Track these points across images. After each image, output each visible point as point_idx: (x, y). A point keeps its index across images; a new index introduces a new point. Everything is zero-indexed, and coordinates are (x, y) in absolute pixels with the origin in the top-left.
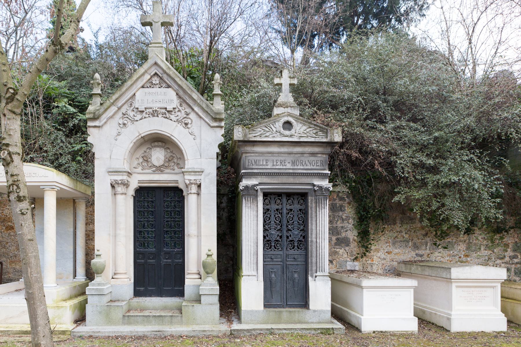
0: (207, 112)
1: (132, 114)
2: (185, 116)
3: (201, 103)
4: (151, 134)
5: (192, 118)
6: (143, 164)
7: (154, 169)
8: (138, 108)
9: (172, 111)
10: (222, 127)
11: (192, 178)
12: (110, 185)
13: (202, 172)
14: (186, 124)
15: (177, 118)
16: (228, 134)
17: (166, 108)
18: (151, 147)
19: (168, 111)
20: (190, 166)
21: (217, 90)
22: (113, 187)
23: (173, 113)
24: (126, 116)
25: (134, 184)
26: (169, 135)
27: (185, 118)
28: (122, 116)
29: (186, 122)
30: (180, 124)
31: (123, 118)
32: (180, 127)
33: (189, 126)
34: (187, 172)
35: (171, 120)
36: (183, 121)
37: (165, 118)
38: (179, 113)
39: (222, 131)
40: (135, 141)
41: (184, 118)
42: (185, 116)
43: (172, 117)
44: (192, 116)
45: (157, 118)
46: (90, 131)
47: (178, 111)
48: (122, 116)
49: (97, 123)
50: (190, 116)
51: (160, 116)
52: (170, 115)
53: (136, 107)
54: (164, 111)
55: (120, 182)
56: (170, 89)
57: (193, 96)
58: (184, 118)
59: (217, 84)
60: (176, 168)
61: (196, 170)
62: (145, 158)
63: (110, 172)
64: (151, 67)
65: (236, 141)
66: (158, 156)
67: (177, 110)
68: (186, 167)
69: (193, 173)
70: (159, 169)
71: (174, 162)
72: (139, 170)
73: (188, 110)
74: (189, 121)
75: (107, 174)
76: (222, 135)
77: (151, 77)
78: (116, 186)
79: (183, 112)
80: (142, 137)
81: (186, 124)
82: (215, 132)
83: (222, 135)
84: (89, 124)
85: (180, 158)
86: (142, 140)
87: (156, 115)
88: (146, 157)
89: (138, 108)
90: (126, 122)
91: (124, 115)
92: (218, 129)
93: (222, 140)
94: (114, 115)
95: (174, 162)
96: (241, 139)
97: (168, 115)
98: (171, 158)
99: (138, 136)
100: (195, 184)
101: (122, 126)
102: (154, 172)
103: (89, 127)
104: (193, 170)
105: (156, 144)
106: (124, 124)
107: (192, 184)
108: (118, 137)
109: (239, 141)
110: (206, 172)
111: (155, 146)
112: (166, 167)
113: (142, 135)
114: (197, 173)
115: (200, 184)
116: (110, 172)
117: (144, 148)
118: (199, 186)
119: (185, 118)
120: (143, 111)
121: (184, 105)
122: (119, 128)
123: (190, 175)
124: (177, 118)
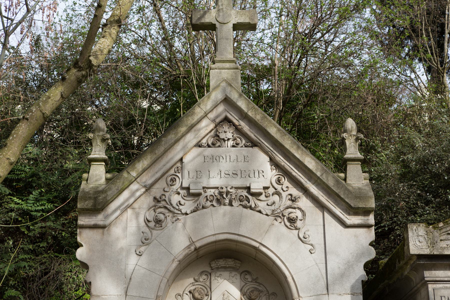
0: (339, 196)
2: (289, 203)
3: (324, 178)
4: (216, 242)
8: (188, 189)
9: (260, 194)
10: (368, 226)
14: (292, 221)
15: (273, 208)
16: (388, 239)
17: (248, 188)
18: (210, 271)
19: (253, 194)
21: (352, 150)
23: (262, 197)
24: (163, 203)
26: (257, 245)
28: (153, 203)
29: (293, 216)
30: (279, 220)
32: (280, 228)
33: (299, 224)
35: (260, 212)
36: (286, 213)
37: (245, 207)
39: (370, 235)
40: (181, 257)
41: (287, 208)
43: (262, 205)
44: (304, 202)
45: (228, 208)
46: (83, 237)
48: (153, 203)
49: (98, 219)
51: (235, 204)
52: (258, 203)
53: (185, 185)
54: (245, 193)
56: (256, 149)
57: (306, 163)
59: (353, 139)
62: (197, 295)
64: (216, 106)
65: (413, 255)
67: (271, 190)
73: (295, 192)
74: (298, 214)
76: (371, 244)
77: (216, 127)
79: (284, 194)
80: (196, 249)
83: (371, 244)
84: (82, 221)
85: (274, 294)
87: (227, 201)
89: (188, 189)
90: (162, 217)
91: (159, 202)
93: (372, 254)
96: (426, 251)
98: (256, 293)
99: (188, 247)
101: (152, 224)
103: (83, 227)
105: (222, 263)
106: (158, 222)
109: (420, 257)
111: (218, 269)
113: (198, 245)
120: (199, 195)
121: (286, 182)
122: (147, 230)
124: (273, 208)
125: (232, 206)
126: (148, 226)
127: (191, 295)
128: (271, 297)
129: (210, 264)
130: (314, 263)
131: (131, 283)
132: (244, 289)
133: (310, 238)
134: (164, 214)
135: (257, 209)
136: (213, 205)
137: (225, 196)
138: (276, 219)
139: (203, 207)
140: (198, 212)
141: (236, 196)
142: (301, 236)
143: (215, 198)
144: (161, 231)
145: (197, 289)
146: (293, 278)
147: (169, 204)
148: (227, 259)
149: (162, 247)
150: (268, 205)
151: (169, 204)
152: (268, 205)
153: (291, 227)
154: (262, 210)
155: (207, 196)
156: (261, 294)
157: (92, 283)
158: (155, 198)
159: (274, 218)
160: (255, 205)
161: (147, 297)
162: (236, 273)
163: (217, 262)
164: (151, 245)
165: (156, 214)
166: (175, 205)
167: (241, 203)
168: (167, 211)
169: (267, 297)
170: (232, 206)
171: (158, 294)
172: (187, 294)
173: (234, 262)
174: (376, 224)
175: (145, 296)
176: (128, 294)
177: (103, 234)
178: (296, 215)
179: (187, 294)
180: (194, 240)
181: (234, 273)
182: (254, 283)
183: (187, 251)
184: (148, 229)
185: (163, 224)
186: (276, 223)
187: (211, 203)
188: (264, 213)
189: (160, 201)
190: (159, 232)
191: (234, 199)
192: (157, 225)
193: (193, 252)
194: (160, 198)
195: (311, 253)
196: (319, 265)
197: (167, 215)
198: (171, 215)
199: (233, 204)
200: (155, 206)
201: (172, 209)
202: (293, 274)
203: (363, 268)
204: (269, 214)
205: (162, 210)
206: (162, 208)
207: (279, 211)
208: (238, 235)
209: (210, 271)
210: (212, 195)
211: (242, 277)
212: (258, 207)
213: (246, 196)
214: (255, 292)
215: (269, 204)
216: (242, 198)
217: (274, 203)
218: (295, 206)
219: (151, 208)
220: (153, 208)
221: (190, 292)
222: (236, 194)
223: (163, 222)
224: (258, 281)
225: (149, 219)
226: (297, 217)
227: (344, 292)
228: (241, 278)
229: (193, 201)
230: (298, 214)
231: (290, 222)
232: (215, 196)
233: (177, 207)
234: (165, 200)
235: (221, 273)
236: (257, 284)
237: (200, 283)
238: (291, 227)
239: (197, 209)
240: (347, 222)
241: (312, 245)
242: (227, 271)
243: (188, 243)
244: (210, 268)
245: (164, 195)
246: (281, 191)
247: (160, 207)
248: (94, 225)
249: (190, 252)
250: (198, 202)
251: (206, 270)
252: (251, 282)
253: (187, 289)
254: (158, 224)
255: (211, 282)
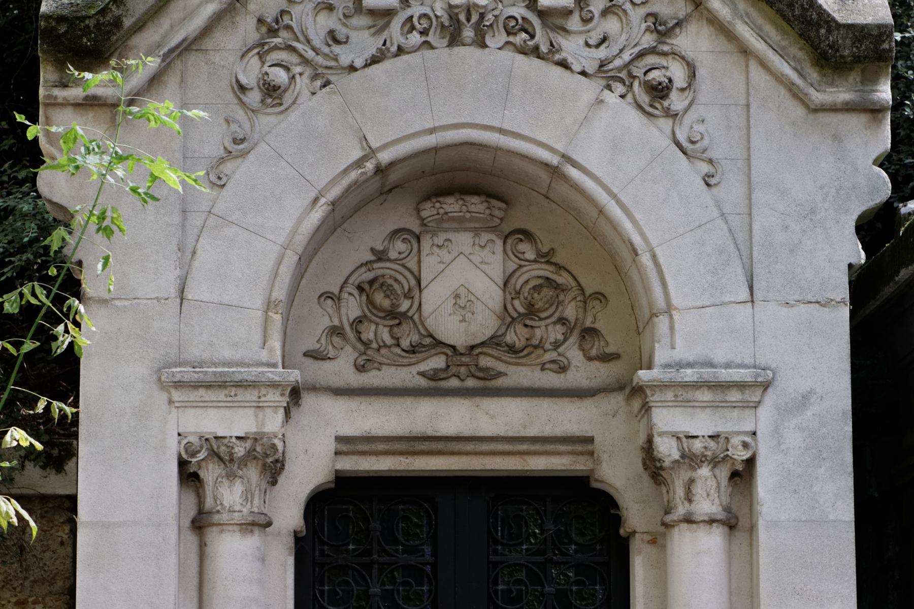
1: (319, 26)
2: (648, 40)
4: (436, 149)
5: (690, 55)
6: (368, 333)
7: (437, 362)
9: (567, 13)
10: (874, 111)
11: (701, 424)
12: (173, 468)
13: (766, 386)
15: (602, 53)
20: (682, 353)
22: (189, 476)
23: (574, 23)
24: (284, 34)
25: (311, 465)
27: (652, 51)
30: (620, 88)
31: (262, 49)
32: (620, 113)
33: (676, 101)
34: (664, 386)
35: (564, 65)
37: (523, 51)
38: (611, 25)
40: (336, 192)
42: (648, 40)
43: (571, 46)
47: (605, 13)
50: (683, 41)
51: (496, 39)
55: (240, 450)
58: (641, 55)
60: (573, 353)
61: (725, 375)
62: (379, 297)
63: (179, 385)
66: (464, 282)
68: (661, 355)
69: (705, 396)
70: (467, 371)
71: (562, 321)
72: (341, 368)
74: (678, 72)
75: (163, 397)
78: (210, 473)
80: (380, 170)
81: (659, 91)
82: (837, 138)
86: (375, 185)
88: (389, 291)
90: (280, 76)
91: (273, 32)
92: (856, 121)
94: (206, 31)
95: (562, 321)
97: (541, 39)
98: (547, 292)
99: (359, 163)
100: (715, 462)
101: (254, 97)
102: (434, 387)
104: (707, 373)
105: (451, 205)
106: (271, 91)
107: (690, 459)
108: (228, 168)
110: (791, 383)
112: (512, 350)
113: (385, 157)
114: (734, 396)
115: (751, 462)
116: (179, 385)
117: (372, 233)
118: (743, 475)
119: (652, 51)
120: (388, 14)
122: (240, 114)
123: (687, 404)
124: (602, 53)
125: (484, 46)
126: (242, 104)
127: (364, 298)
128: (590, 305)
129: (418, 211)
130: (716, 213)
131: (196, 264)
132: (513, 281)
133: (706, 142)
134: (287, 69)
135: (557, 57)
136: (426, 43)
137: (462, 17)
138: (609, 87)
139: (401, 51)
140: (386, 65)
141: (496, 16)
142: (681, 137)
143: (434, 23)
144: (281, 117)
145: (381, 280)
146: (654, 257)
147: (301, 38)
148: (467, 198)
149: (284, 163)
150: (587, 45)
151: (301, 38)
152: (587, 45)
153: (651, 110)
154: (570, 60)
155: (412, 17)
156: (561, 297)
157: (85, 264)
158: (260, 21)
159: (604, 82)
160: (552, 44)
161: (241, 304)
162: (493, 237)
163: (438, 205)
164: (251, 157)
165: (266, 68)
166: (317, 43)
167: (511, 39)
168: (294, 59)
169: (581, 304)
170: (484, 46)
171: (273, 298)
172: (350, 294)
173: (485, 204)
174: (897, 107)
175: (235, 303)
176: (189, 295)
177: (113, 120)
178: (668, 74)
179: (350, 294)
180: (375, 144)
181: (485, 237)
182: (544, 266)
183: (354, 175)
184: (241, 112)
185: (288, 99)
186: (611, 98)
187: (424, 39)
188: (577, 67)
189: (278, 30)
190: (272, 119)
191: (491, 25)
192: (269, 100)
193: (371, 177)
194: (277, 22)
195: (708, 185)
196: (730, 218)
197: (297, 70)
198: (308, 72)
199: (488, 40)
200: (263, 45)
201: (310, 54)
202: (654, 242)
203: (853, 230)
204: (590, 71)
205: (282, 56)
206: (280, 49)
207: (618, 62)
208: (501, 131)
209: (417, 230)
210: (425, 15)
211: (508, 247)
212: (558, 51)
213: (523, 18)
214: (545, 290)
215: (591, 42)
216: (513, 23)
217: (604, 39)
218: (666, 48)
219: (249, 50)
220: (256, 51)
221: (360, 288)
222: (496, 13)
223: (285, 91)
224: (553, 260)
225: (244, 80)
226: (670, 80)
227: (796, 297)
228: (505, 251)
229: (372, 30)
230: (678, 72)
231: (654, 98)
232: (436, 16)
233: (326, 50)
234: (288, 28)
235: (450, 235)
236: (551, 268)
237: (388, 265)
238: (651, 110)
239: (383, 54)
240: (813, 98)
241: (710, 161)
242: (466, 230)
243: (357, 154)
244: (418, 222)
245: (289, 12)
246: (628, 6)
247: (276, 48)
248: (87, 98)
249: (363, 178)
250: (385, 35)
251: (408, 226)
252: (535, 261)
253: (351, 281)
254: (271, 96)
255: (419, 262)
